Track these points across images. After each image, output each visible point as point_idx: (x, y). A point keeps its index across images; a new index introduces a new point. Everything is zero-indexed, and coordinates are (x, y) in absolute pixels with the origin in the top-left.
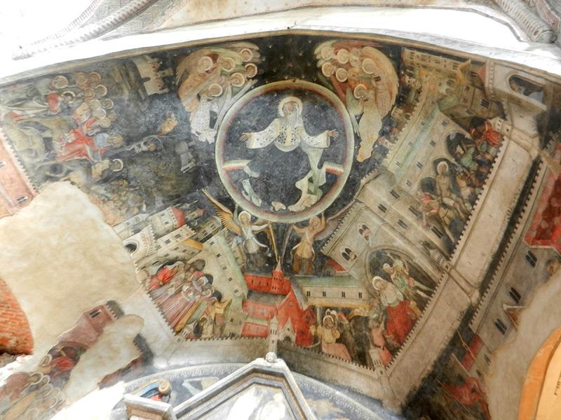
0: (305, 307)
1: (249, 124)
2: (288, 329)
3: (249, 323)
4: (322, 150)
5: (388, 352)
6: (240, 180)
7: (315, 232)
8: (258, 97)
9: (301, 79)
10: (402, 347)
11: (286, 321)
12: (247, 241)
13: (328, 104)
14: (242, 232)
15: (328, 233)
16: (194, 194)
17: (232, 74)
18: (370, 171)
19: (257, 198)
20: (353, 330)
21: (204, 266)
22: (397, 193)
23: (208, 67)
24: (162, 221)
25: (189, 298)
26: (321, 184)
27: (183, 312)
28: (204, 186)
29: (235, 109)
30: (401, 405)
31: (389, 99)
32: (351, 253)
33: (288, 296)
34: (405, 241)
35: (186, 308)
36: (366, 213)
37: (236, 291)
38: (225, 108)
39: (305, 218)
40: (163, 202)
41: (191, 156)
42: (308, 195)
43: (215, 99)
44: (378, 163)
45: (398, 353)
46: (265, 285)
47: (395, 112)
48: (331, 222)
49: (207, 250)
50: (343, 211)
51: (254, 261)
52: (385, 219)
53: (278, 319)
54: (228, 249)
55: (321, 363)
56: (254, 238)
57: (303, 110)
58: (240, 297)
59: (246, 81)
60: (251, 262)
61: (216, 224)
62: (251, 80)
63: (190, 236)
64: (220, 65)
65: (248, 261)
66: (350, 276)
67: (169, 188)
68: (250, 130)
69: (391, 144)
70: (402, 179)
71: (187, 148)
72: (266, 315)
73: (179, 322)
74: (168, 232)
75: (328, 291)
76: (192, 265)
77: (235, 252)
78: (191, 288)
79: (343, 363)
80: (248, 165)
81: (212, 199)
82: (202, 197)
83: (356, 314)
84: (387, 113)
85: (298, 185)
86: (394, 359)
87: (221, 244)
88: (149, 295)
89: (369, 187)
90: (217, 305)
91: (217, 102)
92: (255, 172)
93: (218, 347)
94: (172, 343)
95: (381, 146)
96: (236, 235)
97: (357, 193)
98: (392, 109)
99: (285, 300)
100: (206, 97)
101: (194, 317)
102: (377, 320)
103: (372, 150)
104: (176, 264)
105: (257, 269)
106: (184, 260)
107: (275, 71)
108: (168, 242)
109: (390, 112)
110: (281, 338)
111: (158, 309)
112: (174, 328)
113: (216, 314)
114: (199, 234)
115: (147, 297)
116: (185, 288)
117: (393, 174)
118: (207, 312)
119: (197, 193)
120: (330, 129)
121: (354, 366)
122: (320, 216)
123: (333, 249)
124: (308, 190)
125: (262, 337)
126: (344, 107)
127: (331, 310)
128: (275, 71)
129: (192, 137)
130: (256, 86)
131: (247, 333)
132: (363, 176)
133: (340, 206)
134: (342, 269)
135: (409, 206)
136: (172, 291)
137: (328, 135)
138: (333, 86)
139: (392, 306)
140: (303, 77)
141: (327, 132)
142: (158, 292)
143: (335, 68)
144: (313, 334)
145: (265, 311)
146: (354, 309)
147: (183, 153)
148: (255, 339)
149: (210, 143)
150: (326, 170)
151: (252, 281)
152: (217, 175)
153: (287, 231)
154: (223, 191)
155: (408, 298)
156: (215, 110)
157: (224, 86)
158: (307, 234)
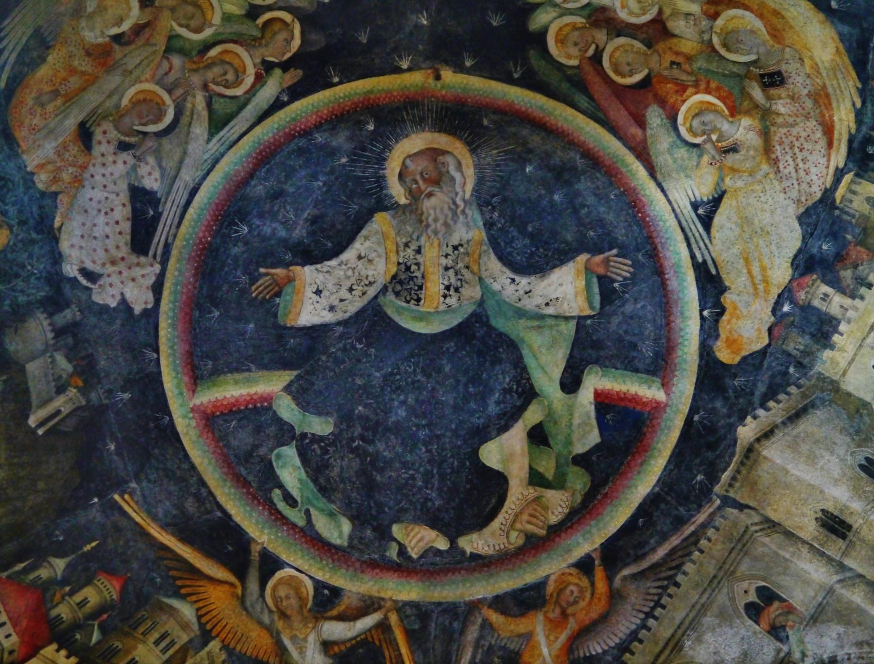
1: (283, 233)
4: (572, 325)
6: (262, 451)
7: (572, 625)
8: (306, 133)
9: (459, 68)
13: (580, 162)
16: (82, 518)
17: (207, 46)
18: (771, 393)
19: (331, 515)
23: (120, 21)
26: (580, 448)
28: (120, 485)
29: (227, 177)
31: (823, 143)
36: (768, 543)
38: (187, 176)
39: (528, 576)
41: (64, 365)
43: (150, 143)
44: (800, 365)
47: (854, 193)
48: (631, 587)
50: (675, 541)
52: (849, 562)
57: (480, 181)
59: (259, 79)
61: (170, 626)
62: (278, 72)
64: (166, 14)
68: (288, 257)
69: (847, 302)
71: (50, 335)
80: (287, 389)
82: (117, 529)
84: (819, 195)
91: (158, 154)
92: (319, 414)
95: (807, 309)
97: (725, 476)
98: (837, 180)
100: (113, 134)
103: (771, 319)
107: (364, 39)
109: (828, 195)
119: (94, 513)
120: (596, 249)
122: (585, 566)
126: (641, 172)
128: (364, 39)
129: (67, 289)
130: (296, 93)
132: (742, 419)
133: (664, 524)
137: (588, 269)
138: (591, 98)
140: (468, 63)
141: (583, 258)
143: (601, 36)
147: (33, 358)
149: (138, 309)
150: (598, 394)
152: (171, 435)
153: (462, 632)
154: (198, 497)
156: (152, 182)
157: (179, 92)
158: (541, 637)
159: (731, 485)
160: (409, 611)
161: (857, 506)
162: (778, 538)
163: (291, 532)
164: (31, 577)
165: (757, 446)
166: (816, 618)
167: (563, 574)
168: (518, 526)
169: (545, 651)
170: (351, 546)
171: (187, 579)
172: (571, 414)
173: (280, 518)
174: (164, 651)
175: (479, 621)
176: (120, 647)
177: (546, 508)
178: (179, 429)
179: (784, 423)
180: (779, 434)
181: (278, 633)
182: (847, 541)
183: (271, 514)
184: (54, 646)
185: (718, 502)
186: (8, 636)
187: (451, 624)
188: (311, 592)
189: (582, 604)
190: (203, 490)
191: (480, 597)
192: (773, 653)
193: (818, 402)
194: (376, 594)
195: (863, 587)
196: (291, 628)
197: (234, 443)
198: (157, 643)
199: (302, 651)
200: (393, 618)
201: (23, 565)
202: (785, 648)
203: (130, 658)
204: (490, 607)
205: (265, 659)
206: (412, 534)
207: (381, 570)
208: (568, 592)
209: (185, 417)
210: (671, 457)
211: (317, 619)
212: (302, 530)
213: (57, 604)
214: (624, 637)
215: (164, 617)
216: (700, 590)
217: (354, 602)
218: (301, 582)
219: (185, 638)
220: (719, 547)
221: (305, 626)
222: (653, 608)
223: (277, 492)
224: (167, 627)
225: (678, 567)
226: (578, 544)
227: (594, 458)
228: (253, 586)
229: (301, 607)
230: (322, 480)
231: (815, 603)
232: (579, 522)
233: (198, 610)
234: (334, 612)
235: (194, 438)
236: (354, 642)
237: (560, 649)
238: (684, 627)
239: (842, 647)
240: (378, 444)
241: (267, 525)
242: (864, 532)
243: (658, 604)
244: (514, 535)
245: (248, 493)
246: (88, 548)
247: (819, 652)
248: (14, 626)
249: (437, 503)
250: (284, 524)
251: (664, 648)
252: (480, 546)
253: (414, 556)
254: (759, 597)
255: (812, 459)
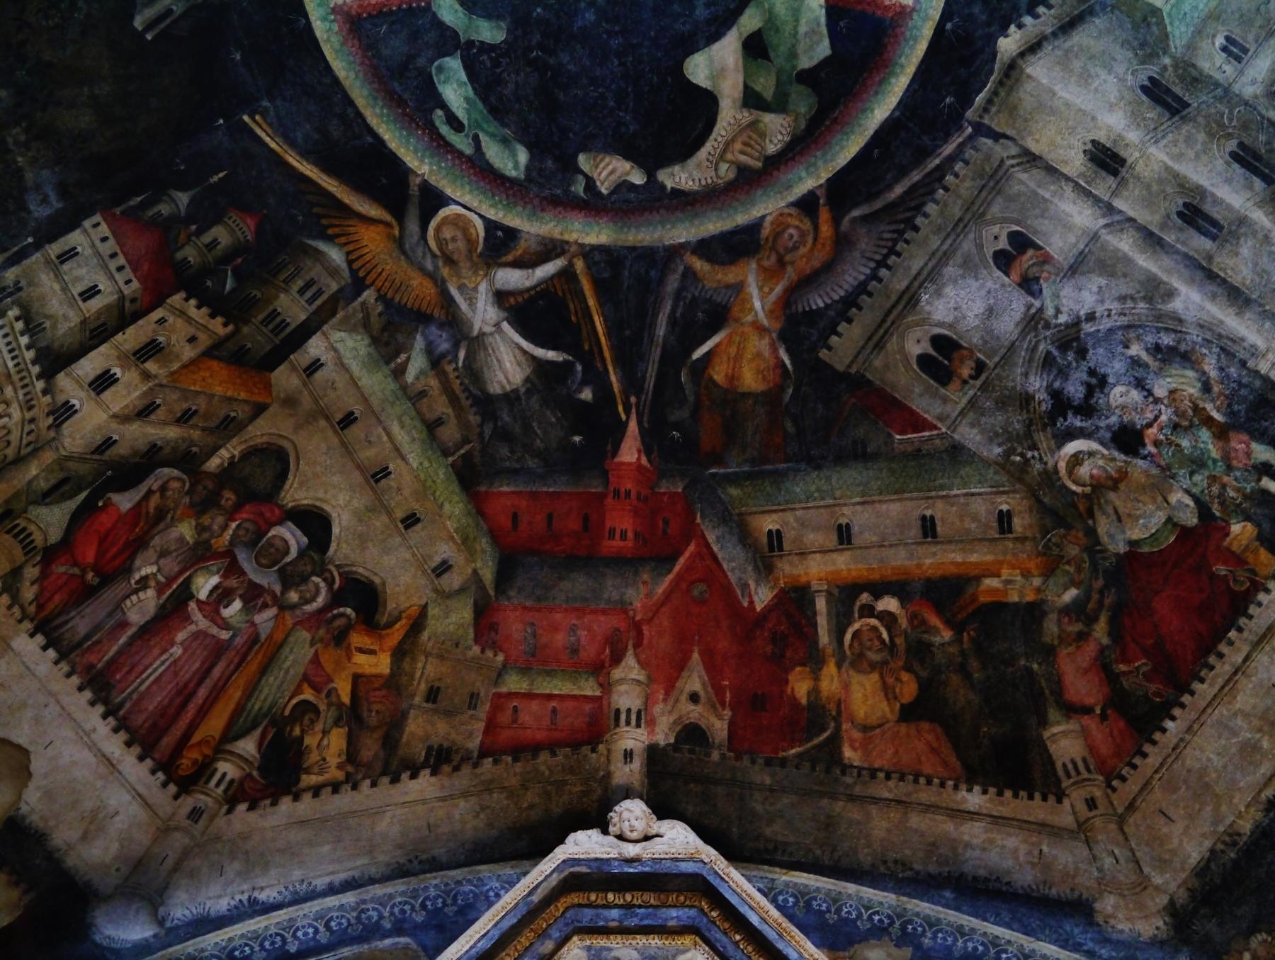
0: (762, 597)
2: (694, 698)
3: (511, 695)
5: (1122, 724)
6: (421, 62)
7: (791, 274)
10: (1186, 699)
11: (680, 666)
12: (477, 343)
14: (448, 301)
15: (852, 274)
19: (504, 141)
20: (974, 664)
21: (282, 475)
22: (1177, 90)
24: (65, 289)
25: (225, 625)
26: (805, 63)
27: (202, 693)
30: (1172, 902)
32: (956, 355)
33: (682, 560)
34: (1214, 288)
35: (216, 672)
36: (1026, 180)
37: (444, 568)
39: (742, 218)
40: (63, 190)
42: (746, 116)
45: (1169, 724)
46: (574, 524)
48: (862, 231)
49: (290, 402)
50: (916, 176)
51: (517, 429)
53: (643, 664)
54: (392, 385)
55: (839, 806)
56: (505, 325)
58: (462, 590)
60: (504, 435)
61: (316, 271)
63: (204, 341)
65: (488, 430)
66: (956, 453)
67: (85, 120)
70: (1199, 32)
72: (589, 652)
73: (187, 735)
74: (97, 334)
75: (858, 517)
76: (228, 474)
77: (423, 394)
78: (233, 582)
79: (926, 795)
81: (293, 160)
83: (983, 599)
85: (699, 69)
86: (1147, 748)
87: (355, 368)
88: (40, 639)
89: (1039, 70)
90: (358, 639)
92: (488, 16)
93: (378, 812)
94: (165, 830)
96: (422, 318)
97: (980, 99)
99: (671, 576)
101: (256, 705)
102: (1076, 611)
104: (152, 482)
105: (531, 463)
106: (187, 460)
108: (103, 382)
110: (663, 735)
111: (88, 694)
112: (166, 766)
113: (357, 679)
114: (246, 330)
115: (28, 645)
116: (205, 585)
117: (1156, 11)
118: (315, 677)
121: (974, 799)
122: (807, 205)
123: (877, 340)
124: (746, 86)
125: (575, 745)
127: (877, 596)
131: (505, 736)
132: (1003, 31)
134: (917, 423)
135: (1232, 145)
136: (143, 606)
139: (1145, 549)
142: (80, 624)
144: (804, 701)
145: (582, 634)
146: (978, 579)
148: (544, 756)
151: (515, 516)
153: (661, 282)
155: (1216, 510)
158: (753, 290)
159: (986, 110)
160: (597, 257)
161: (1133, 136)
162: (1037, 174)
163: (457, 162)
164: (150, 213)
165: (1020, 62)
166: (1075, 269)
167: (781, 215)
168: (729, 156)
169: (757, 304)
170: (529, 178)
171: (335, 217)
172: (797, 20)
173: (441, 146)
174: (310, 301)
175: (681, 268)
176: (259, 295)
177: (763, 135)
178: (318, 34)
179: (1054, 34)
180: (1048, 48)
181: (444, 281)
182: (1119, 179)
183: (432, 140)
184: (182, 295)
185: (970, 129)
186: (128, 282)
187: (647, 272)
188: (482, 234)
189: (803, 251)
190: (350, 110)
191: (682, 240)
192: (1023, 309)
193: (1097, 8)
194: (559, 237)
195: (1132, 232)
196: (459, 276)
197: (386, 52)
198: (302, 292)
199: (472, 302)
200: (579, 265)
201: (139, 199)
202: (1037, 304)
203: (271, 308)
204: (694, 252)
205: (429, 312)
206: (602, 165)
207: (565, 208)
208: (786, 236)
209: (324, 19)
210: (915, 74)
211: (489, 266)
212: (469, 159)
213: (182, 247)
214: (850, 290)
215: (309, 263)
216: (944, 234)
217: (534, 246)
218: (470, 221)
219: (334, 287)
220: (967, 184)
221: (476, 273)
222: (886, 257)
223: (439, 112)
224: (313, 274)
225: (918, 209)
226: (800, 179)
227: (822, 75)
228: (413, 226)
229: (470, 251)
230: (493, 99)
231: (1075, 251)
232: (801, 153)
233: (348, 253)
234: (510, 258)
235: (337, 46)
236: (533, 292)
237: (775, 303)
238: (921, 278)
239: (1102, 302)
240: (562, 55)
241: (427, 153)
242: (1140, 167)
243: (892, 251)
244: (724, 167)
245: (404, 114)
246: (215, 178)
247: (1076, 308)
248: (135, 270)
249: (632, 128)
250: (448, 152)
251: (897, 302)
252: (683, 181)
253: (604, 191)
254: (1010, 244)
255: (1085, 78)
